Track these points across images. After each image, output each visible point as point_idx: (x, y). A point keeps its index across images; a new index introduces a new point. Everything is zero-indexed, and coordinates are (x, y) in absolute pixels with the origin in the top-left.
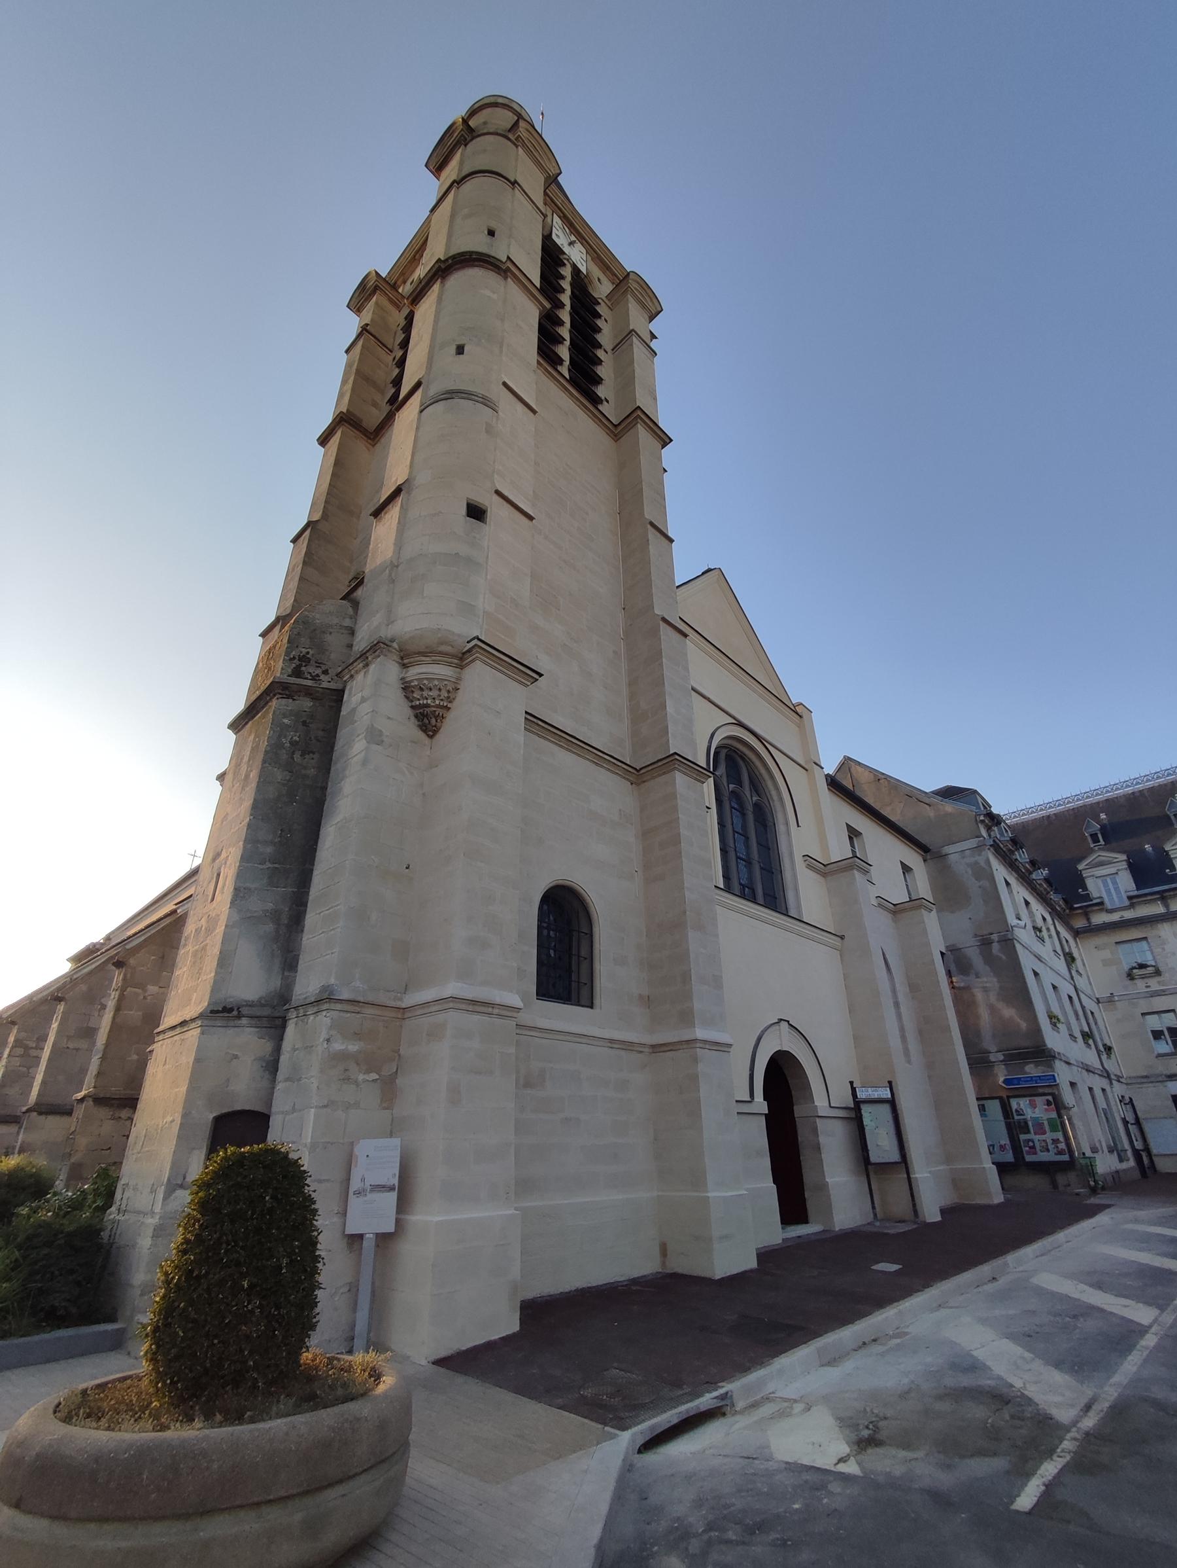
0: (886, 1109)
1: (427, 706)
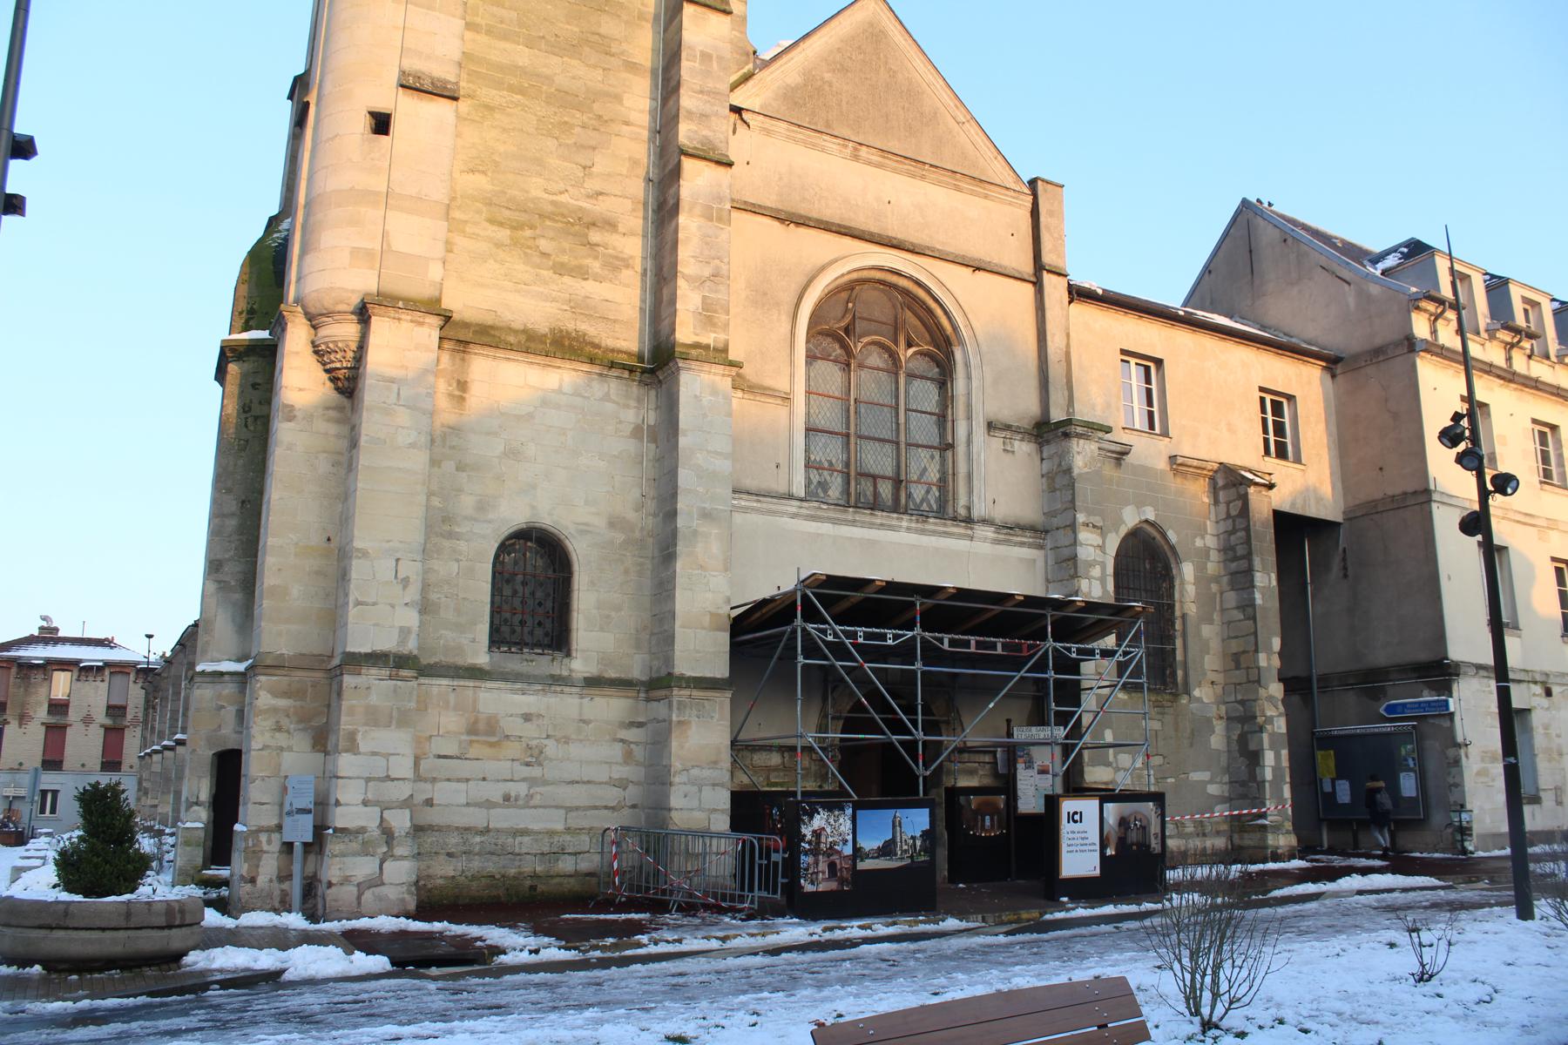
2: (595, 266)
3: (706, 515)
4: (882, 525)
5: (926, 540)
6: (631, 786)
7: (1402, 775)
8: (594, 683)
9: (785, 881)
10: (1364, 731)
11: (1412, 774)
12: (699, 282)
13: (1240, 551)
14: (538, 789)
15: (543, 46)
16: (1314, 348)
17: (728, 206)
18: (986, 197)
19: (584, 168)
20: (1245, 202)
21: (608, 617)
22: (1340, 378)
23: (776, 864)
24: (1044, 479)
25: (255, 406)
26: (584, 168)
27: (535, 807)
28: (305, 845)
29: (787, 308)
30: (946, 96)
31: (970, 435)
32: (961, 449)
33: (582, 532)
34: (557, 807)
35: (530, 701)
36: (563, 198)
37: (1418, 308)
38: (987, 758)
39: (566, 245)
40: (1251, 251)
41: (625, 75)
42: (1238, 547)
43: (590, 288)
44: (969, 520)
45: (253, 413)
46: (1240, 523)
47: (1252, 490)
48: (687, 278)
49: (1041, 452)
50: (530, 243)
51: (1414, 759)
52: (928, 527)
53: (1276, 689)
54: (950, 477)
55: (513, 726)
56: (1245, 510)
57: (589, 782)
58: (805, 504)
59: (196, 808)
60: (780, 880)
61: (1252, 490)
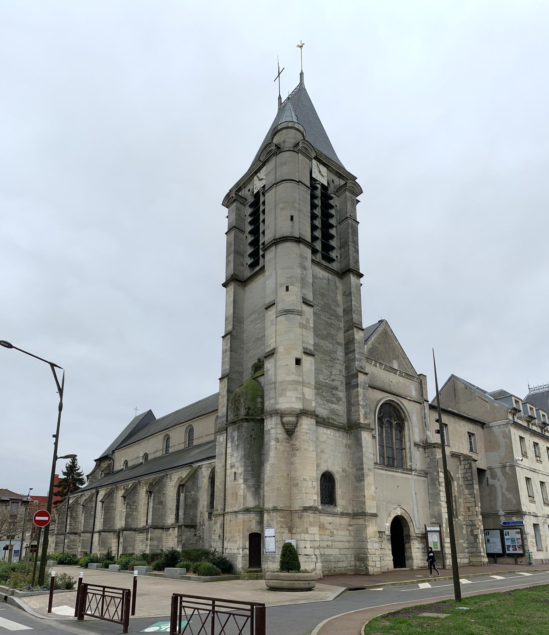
0: (438, 533)
1: (289, 429)
3: (369, 469)
6: (351, 543)
12: (364, 407)
14: (333, 543)
15: (320, 337)
17: (368, 386)
19: (330, 372)
21: (344, 496)
26: (330, 372)
27: (333, 548)
29: (373, 412)
35: (330, 519)
36: (327, 381)
39: (328, 394)
41: (337, 346)
43: (334, 406)
48: (361, 405)
50: (321, 393)
52: (404, 472)
55: (328, 526)
57: (343, 541)
58: (380, 466)
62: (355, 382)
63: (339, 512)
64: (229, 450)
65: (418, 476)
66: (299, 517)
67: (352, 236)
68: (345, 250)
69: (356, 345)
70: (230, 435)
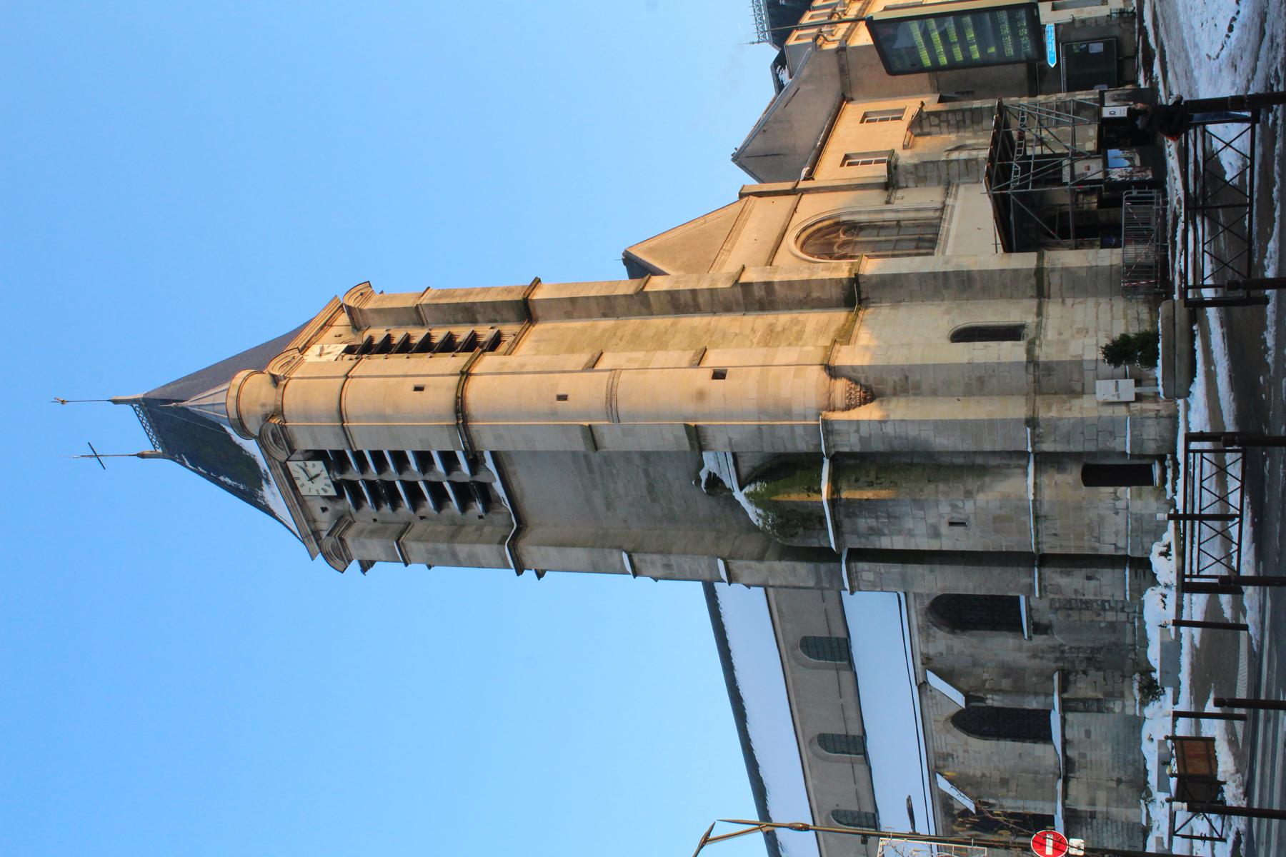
2: (795, 328)
3: (947, 263)
4: (947, 233)
5: (955, 220)
7: (1091, 52)
8: (1039, 313)
9: (1147, 188)
10: (1065, 76)
11: (1090, 45)
13: (959, 117)
14: (1101, 328)
16: (826, 127)
18: (751, 211)
20: (733, 160)
22: (854, 96)
23: (1139, 193)
24: (918, 185)
25: (869, 480)
28: (1136, 385)
30: (688, 227)
31: (893, 211)
32: (900, 216)
33: (953, 322)
34: (1112, 322)
37: (821, 46)
38: (1081, 197)
40: (766, 155)
41: (679, 326)
42: (958, 119)
44: (942, 209)
45: (874, 480)
46: (943, 117)
47: (925, 110)
49: (902, 188)
51: (1081, 44)
52: (947, 218)
53: (1041, 98)
54: (917, 222)
56: (936, 114)
57: (1097, 314)
59: (1118, 494)
60: (1147, 190)
61: (925, 110)
62: (760, 288)
63: (1036, 320)
64: (898, 543)
65: (956, 198)
66: (1050, 375)
67: (453, 297)
68: (482, 310)
69: (681, 287)
70: (863, 540)
